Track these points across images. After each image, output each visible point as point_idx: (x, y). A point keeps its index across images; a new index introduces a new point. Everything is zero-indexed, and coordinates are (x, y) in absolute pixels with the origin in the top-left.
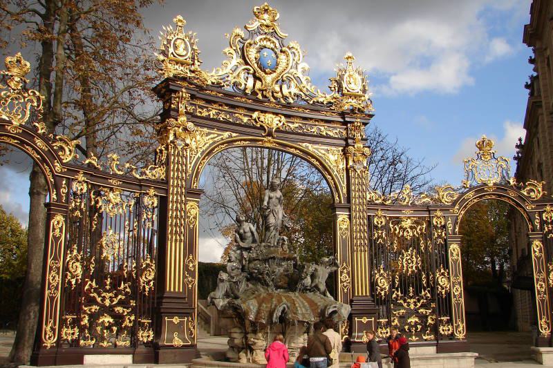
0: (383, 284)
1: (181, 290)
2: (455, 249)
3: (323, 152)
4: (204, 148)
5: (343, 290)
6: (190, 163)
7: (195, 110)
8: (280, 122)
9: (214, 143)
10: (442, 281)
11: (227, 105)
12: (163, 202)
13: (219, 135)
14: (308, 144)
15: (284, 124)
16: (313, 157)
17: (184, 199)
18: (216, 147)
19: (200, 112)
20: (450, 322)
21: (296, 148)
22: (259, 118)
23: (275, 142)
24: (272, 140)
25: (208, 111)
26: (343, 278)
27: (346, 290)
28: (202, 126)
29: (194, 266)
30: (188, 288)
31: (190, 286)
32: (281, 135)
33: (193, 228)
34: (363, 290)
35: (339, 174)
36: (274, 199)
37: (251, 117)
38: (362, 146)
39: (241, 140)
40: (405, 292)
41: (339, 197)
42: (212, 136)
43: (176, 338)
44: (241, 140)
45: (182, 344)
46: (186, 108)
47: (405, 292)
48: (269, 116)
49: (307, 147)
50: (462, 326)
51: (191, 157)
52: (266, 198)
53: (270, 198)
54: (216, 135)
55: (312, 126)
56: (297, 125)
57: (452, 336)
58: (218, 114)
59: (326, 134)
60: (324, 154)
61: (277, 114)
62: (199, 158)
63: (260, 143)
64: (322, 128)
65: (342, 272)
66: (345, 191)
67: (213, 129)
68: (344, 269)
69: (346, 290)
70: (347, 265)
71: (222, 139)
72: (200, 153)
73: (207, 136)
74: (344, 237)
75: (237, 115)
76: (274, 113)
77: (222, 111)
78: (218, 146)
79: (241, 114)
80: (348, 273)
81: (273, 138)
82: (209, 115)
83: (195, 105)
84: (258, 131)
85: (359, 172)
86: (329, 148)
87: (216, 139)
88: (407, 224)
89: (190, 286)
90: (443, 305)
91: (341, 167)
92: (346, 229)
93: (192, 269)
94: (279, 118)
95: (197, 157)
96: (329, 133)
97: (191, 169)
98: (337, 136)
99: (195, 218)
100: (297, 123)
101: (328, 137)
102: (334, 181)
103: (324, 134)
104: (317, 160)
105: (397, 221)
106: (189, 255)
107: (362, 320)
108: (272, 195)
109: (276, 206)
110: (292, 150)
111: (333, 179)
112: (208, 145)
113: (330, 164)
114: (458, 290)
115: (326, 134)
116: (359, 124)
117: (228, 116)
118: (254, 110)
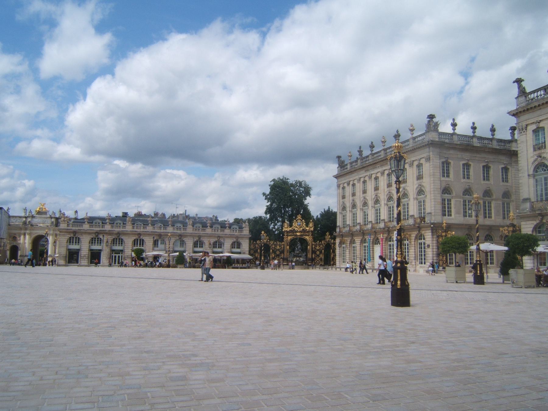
0: (313, 256)
2: (323, 251)
10: (321, 256)
12: (284, 247)
20: (322, 262)
26: (308, 255)
34: (310, 257)
40: (317, 257)
47: (317, 257)
48: (298, 233)
50: (323, 262)
57: (322, 264)
88: (318, 247)
90: (321, 259)
101: (307, 235)
105: (317, 247)
114: (323, 257)
118: (296, 233)
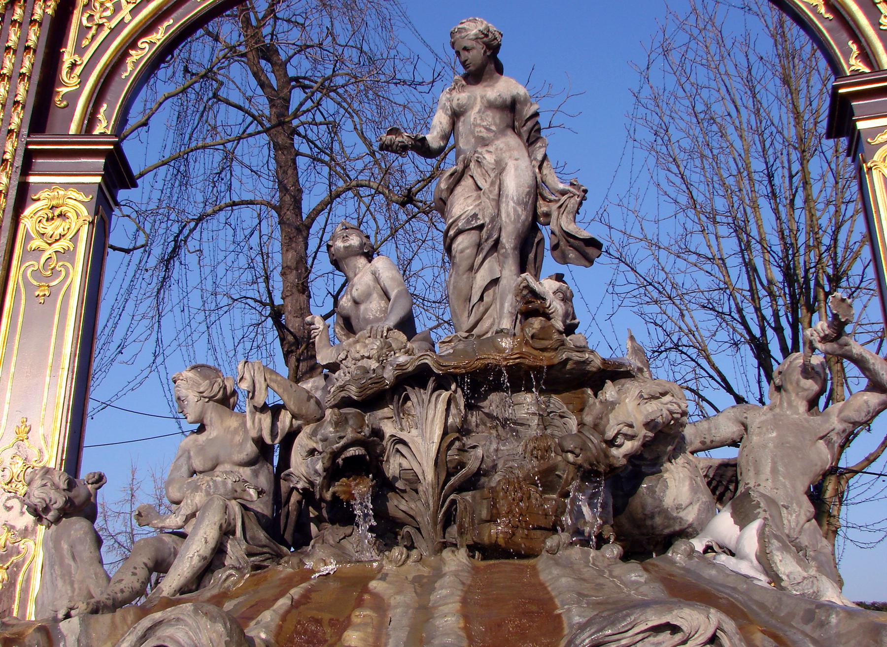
6: (80, 50)
36: (473, 115)
51: (83, 31)
53: (456, 115)
97: (78, 70)
108: (462, 97)
109: (484, 142)
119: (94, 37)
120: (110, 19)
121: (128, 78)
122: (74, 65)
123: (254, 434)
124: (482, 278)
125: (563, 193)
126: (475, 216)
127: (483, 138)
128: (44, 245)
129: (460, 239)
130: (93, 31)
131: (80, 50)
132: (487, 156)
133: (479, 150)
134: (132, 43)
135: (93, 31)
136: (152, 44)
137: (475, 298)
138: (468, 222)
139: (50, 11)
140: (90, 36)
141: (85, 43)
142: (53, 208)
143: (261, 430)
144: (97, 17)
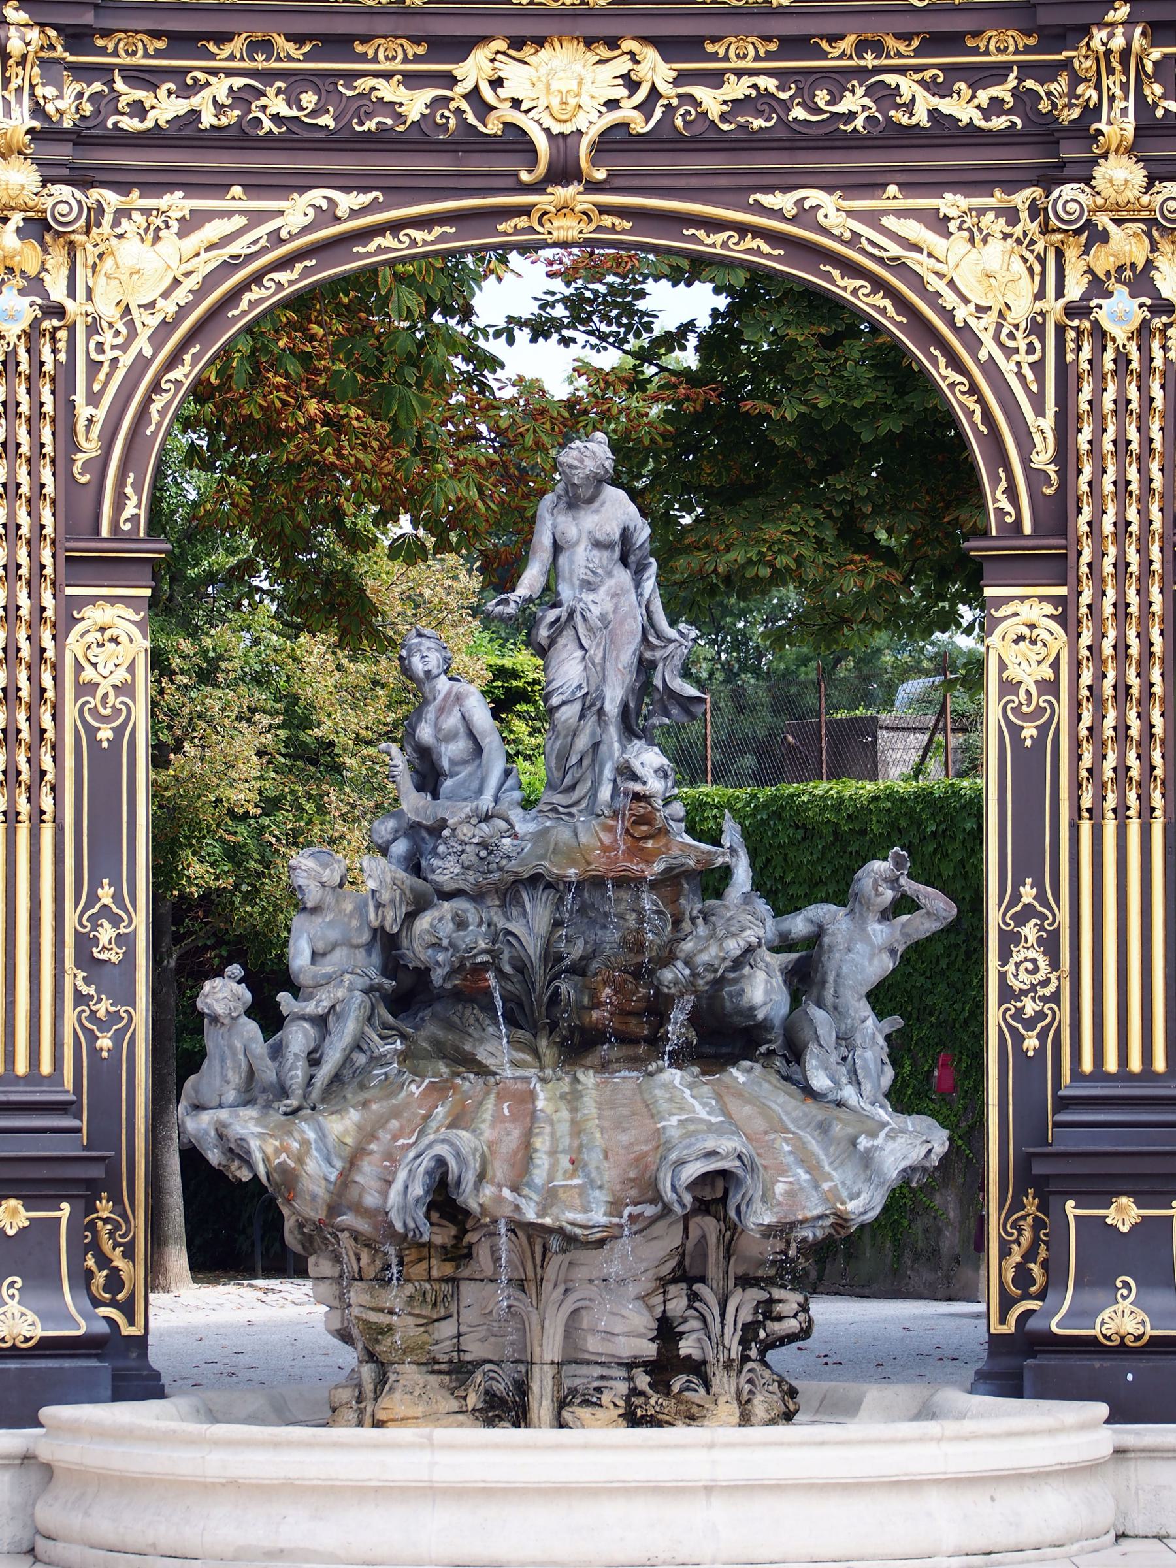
1: (46, 1068)
3: (912, 229)
4: (168, 308)
5: (1019, 1039)
6: (93, 399)
7: (106, 102)
8: (632, 85)
9: (229, 267)
11: (297, 39)
13: (257, 218)
14: (815, 197)
15: (654, 93)
16: (852, 269)
17: (48, 600)
18: (244, 287)
19: (139, 110)
21: (743, 230)
22: (496, 83)
23: (604, 210)
24: (586, 201)
25: (187, 91)
27: (1031, 1043)
28: (155, 185)
29: (125, 941)
30: (94, 1052)
31: (105, 1043)
32: (627, 165)
33: (116, 742)
35: (1009, 352)
37: (451, 80)
38: (1139, 175)
39: (395, 227)
41: (1012, 493)
42: (214, 230)
43: (13, 1306)
44: (395, 227)
45: (38, 1332)
46: (38, 111)
49: (805, 216)
51: (94, 366)
52: (543, 540)
54: (239, 221)
55: (838, 80)
56: (737, 89)
58: (241, 98)
59: (933, 113)
60: (918, 249)
61: (612, 43)
62: (142, 363)
63: (522, 222)
64: (907, 86)
65: (1009, 940)
66: (1043, 457)
67: (221, 189)
68: (1022, 918)
69: (1031, 1043)
70: (1041, 897)
71: (276, 239)
72: (144, 335)
73: (181, 235)
74: (1029, 732)
75: (363, 84)
76: (589, 42)
77: (268, 76)
78: (257, 279)
79: (387, 75)
80: (1050, 944)
81: (594, 187)
82: (195, 114)
83: (110, 69)
84: (499, 163)
85: (1119, 332)
86: (951, 203)
87: (237, 248)
89: (105, 1043)
91: (1021, 310)
92: (1049, 687)
93: (115, 959)
94: (622, 65)
95: (126, 360)
96: (947, 106)
98: (999, 123)
99: (125, 689)
100: (740, 73)
102: (981, 401)
103: (921, 117)
104: (879, 284)
106: (95, 884)
107: (1112, 1215)
109: (588, 586)
110: (712, 243)
111: (974, 389)
112: (191, 283)
113: (950, 300)
115: (933, 113)
116: (1118, 43)
117: (309, 100)
118: (462, 47)
119: (109, 376)
120: (124, 347)
121: (156, 433)
122: (90, 421)
123: (375, 924)
124: (582, 742)
125: (671, 641)
126: (580, 687)
127: (589, 583)
128: (98, 679)
129: (563, 709)
130: (106, 369)
131: (93, 399)
132: (592, 607)
133: (584, 596)
134: (156, 388)
135: (106, 369)
136: (178, 383)
137: (574, 760)
138: (573, 693)
139: (62, 357)
140: (102, 376)
141: (97, 387)
142: (102, 629)
143: (383, 920)
144: (107, 347)
